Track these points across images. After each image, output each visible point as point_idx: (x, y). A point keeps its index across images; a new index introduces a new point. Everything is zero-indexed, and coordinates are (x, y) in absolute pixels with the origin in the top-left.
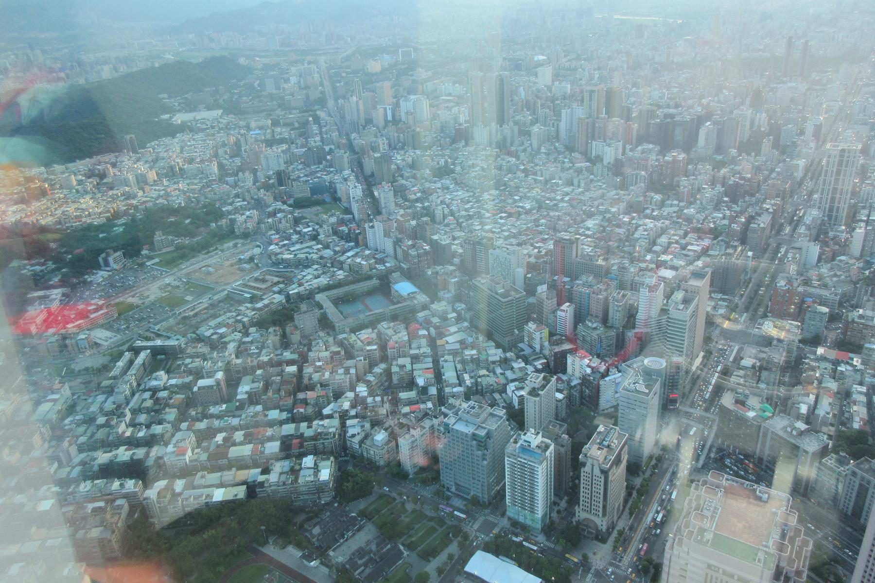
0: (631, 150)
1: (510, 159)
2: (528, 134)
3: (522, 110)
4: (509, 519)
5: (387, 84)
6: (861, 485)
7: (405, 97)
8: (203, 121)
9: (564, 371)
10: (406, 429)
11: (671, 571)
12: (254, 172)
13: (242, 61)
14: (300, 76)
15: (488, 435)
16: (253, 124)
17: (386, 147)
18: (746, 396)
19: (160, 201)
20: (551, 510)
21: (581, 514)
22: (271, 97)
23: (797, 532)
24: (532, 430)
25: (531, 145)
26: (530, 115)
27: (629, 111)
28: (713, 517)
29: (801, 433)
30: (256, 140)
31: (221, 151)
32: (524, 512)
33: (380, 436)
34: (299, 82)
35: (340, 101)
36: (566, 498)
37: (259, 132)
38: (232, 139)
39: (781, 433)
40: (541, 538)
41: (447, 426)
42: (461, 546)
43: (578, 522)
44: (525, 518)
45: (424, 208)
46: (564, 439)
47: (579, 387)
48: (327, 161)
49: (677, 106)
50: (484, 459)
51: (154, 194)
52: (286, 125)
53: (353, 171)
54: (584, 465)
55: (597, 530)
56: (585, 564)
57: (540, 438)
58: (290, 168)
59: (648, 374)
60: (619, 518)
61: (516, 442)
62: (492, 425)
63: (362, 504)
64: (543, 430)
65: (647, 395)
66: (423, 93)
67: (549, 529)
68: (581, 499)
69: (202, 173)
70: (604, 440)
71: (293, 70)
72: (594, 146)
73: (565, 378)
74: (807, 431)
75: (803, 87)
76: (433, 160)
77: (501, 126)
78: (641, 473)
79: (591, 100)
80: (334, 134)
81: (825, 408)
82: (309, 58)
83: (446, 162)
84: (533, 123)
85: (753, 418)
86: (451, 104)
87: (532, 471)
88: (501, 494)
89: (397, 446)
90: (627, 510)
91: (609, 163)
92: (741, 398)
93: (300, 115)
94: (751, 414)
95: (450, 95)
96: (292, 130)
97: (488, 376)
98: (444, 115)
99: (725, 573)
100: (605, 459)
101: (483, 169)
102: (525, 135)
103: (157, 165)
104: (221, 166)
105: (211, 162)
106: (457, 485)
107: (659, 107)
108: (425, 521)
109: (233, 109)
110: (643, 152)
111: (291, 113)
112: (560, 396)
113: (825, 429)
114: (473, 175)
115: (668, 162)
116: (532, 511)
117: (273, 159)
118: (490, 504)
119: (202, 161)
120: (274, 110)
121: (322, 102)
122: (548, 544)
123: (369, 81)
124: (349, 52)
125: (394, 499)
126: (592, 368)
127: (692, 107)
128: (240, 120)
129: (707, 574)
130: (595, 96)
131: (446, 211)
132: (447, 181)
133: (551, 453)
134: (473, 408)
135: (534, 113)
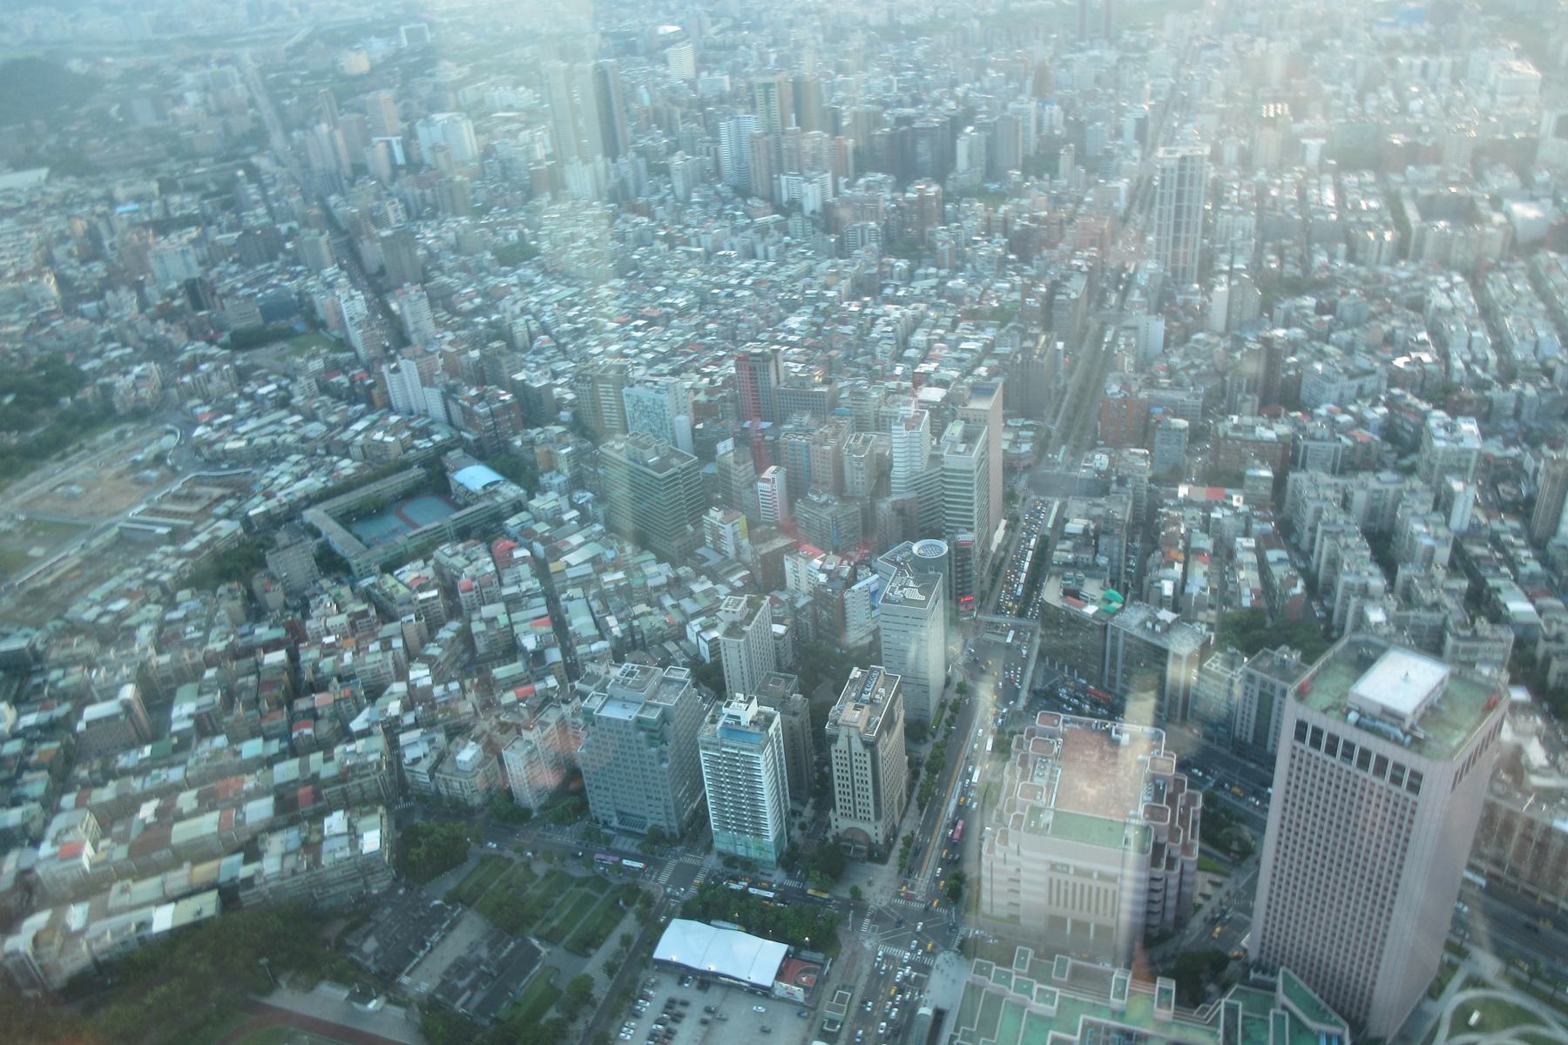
0: (848, 186)
1: (638, 220)
2: (664, 171)
3: (649, 128)
4: (720, 854)
5: (386, 95)
6: (1261, 693)
7: (425, 117)
9: (782, 586)
10: (513, 732)
11: (995, 887)
12: (139, 287)
13: (75, 65)
14: (206, 89)
15: (665, 718)
16: (120, 193)
17: (402, 216)
18: (1080, 582)
20: (790, 825)
21: (840, 823)
22: (152, 135)
23: (1179, 785)
24: (741, 696)
25: (672, 190)
26: (665, 136)
27: (837, 117)
28: (1050, 786)
29: (1168, 628)
30: (132, 225)
31: (59, 253)
32: (743, 838)
33: (468, 754)
34: (205, 102)
36: (811, 800)
38: (80, 226)
39: (1137, 632)
40: (779, 876)
41: (588, 714)
42: (642, 918)
43: (837, 838)
44: (748, 847)
46: (796, 701)
47: (809, 609)
48: (287, 252)
49: (916, 102)
50: (663, 760)
52: (191, 188)
53: (341, 267)
54: (834, 739)
55: (870, 844)
56: (857, 905)
57: (754, 707)
58: (213, 273)
59: (921, 568)
60: (903, 816)
61: (714, 721)
62: (670, 700)
63: (450, 882)
64: (759, 692)
65: (923, 604)
66: (458, 108)
67: (789, 859)
68: (837, 797)
69: (25, 299)
70: (863, 692)
71: (189, 78)
72: (784, 183)
73: (784, 597)
74: (1176, 621)
75: (1111, 56)
76: (495, 233)
77: (614, 161)
78: (929, 737)
79: (767, 100)
80: (293, 200)
81: (1199, 582)
82: (218, 53)
83: (521, 234)
84: (671, 151)
85: (1094, 616)
86: (515, 126)
87: (750, 766)
88: (701, 817)
89: (501, 761)
90: (914, 801)
91: (813, 212)
92: (1072, 585)
93: (218, 167)
94: (1090, 610)
95: (509, 108)
96: (205, 197)
97: (650, 614)
98: (505, 147)
99: (1078, 872)
100: (869, 722)
101: (591, 243)
102: (658, 174)
104: (63, 282)
105: (41, 274)
106: (620, 813)
107: (886, 106)
108: (572, 888)
109: (68, 163)
110: (868, 187)
111: (197, 165)
112: (779, 629)
113: (1202, 616)
114: (574, 254)
115: (911, 202)
116: (758, 833)
117: (174, 258)
118: (683, 835)
119: (20, 276)
120: (163, 160)
121: (258, 137)
122: (789, 883)
123: (349, 91)
124: (300, 36)
125: (510, 861)
126: (828, 573)
127: (938, 102)
128: (92, 185)
129: (1051, 881)
130: (775, 91)
131: (534, 326)
132: (527, 272)
133: (776, 730)
134: (631, 674)
135: (670, 132)
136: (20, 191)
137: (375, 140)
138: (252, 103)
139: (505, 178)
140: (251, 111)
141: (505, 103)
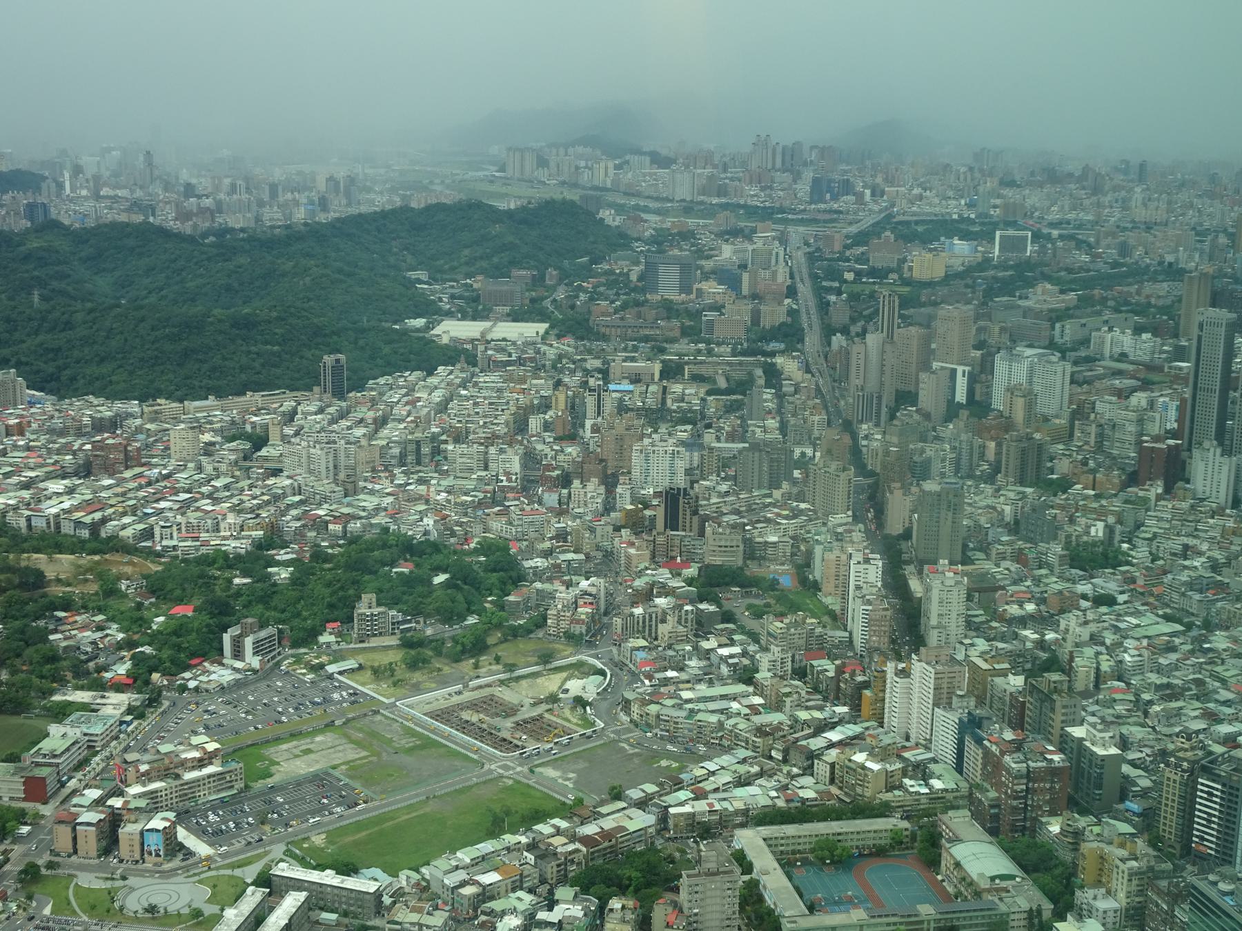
8: (502, 345)
12: (610, 482)
17: (949, 469)
19: (381, 519)
22: (669, 309)
31: (534, 423)
35: (838, 340)
37: (631, 387)
45: (1041, 644)
48: (794, 482)
51: (369, 502)
52: (697, 378)
69: (486, 468)
80: (816, 418)
96: (709, 393)
101: (1215, 567)
103: (385, 432)
104: (530, 459)
114: (1184, 577)
119: (491, 440)
120: (673, 341)
121: (790, 335)
128: (590, 352)
131: (1106, 666)
136: (514, 343)
137: (936, 365)
138: (792, 292)
139: (1099, 447)
140: (787, 301)
141: (1117, 350)
